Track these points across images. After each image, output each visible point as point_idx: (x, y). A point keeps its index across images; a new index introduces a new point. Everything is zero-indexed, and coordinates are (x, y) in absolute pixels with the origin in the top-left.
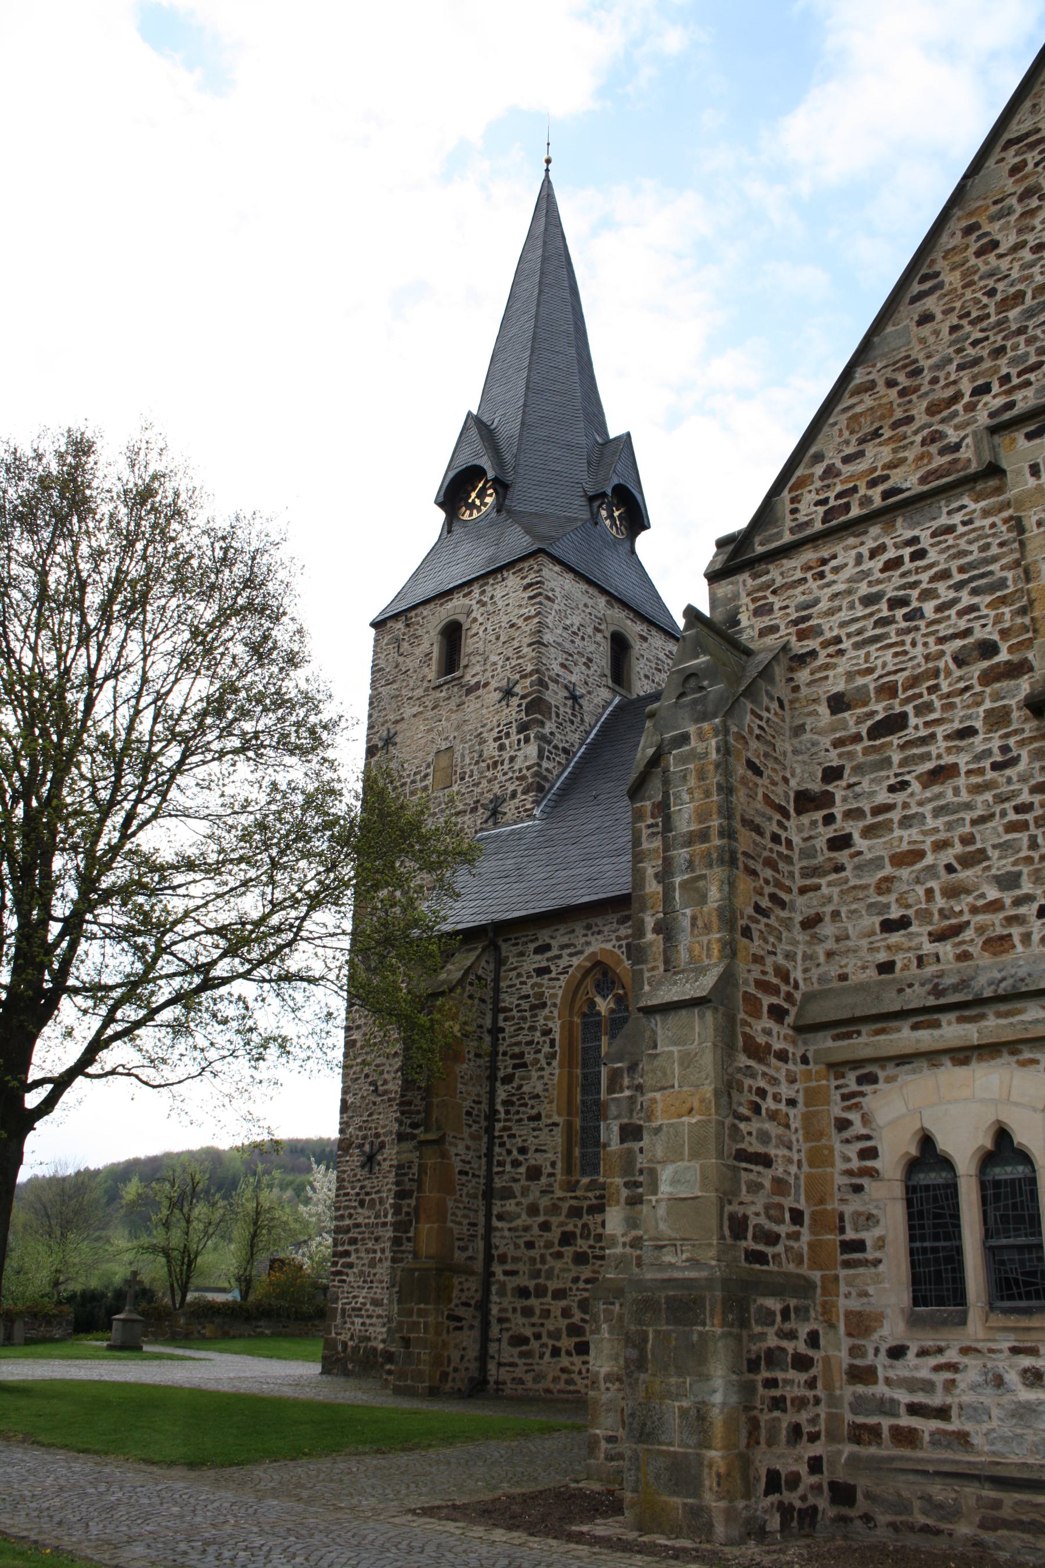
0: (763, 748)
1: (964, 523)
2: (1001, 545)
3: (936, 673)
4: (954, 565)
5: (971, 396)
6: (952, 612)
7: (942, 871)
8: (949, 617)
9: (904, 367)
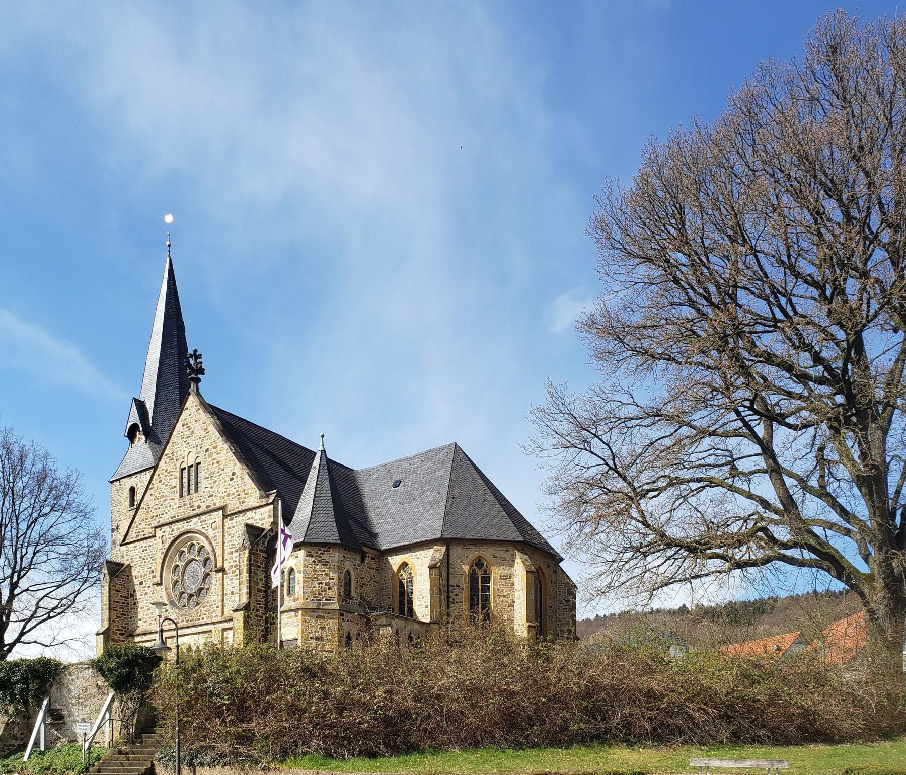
0: (120, 586)
4: (151, 553)
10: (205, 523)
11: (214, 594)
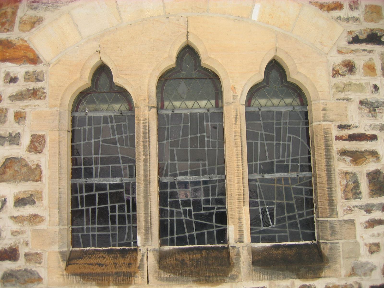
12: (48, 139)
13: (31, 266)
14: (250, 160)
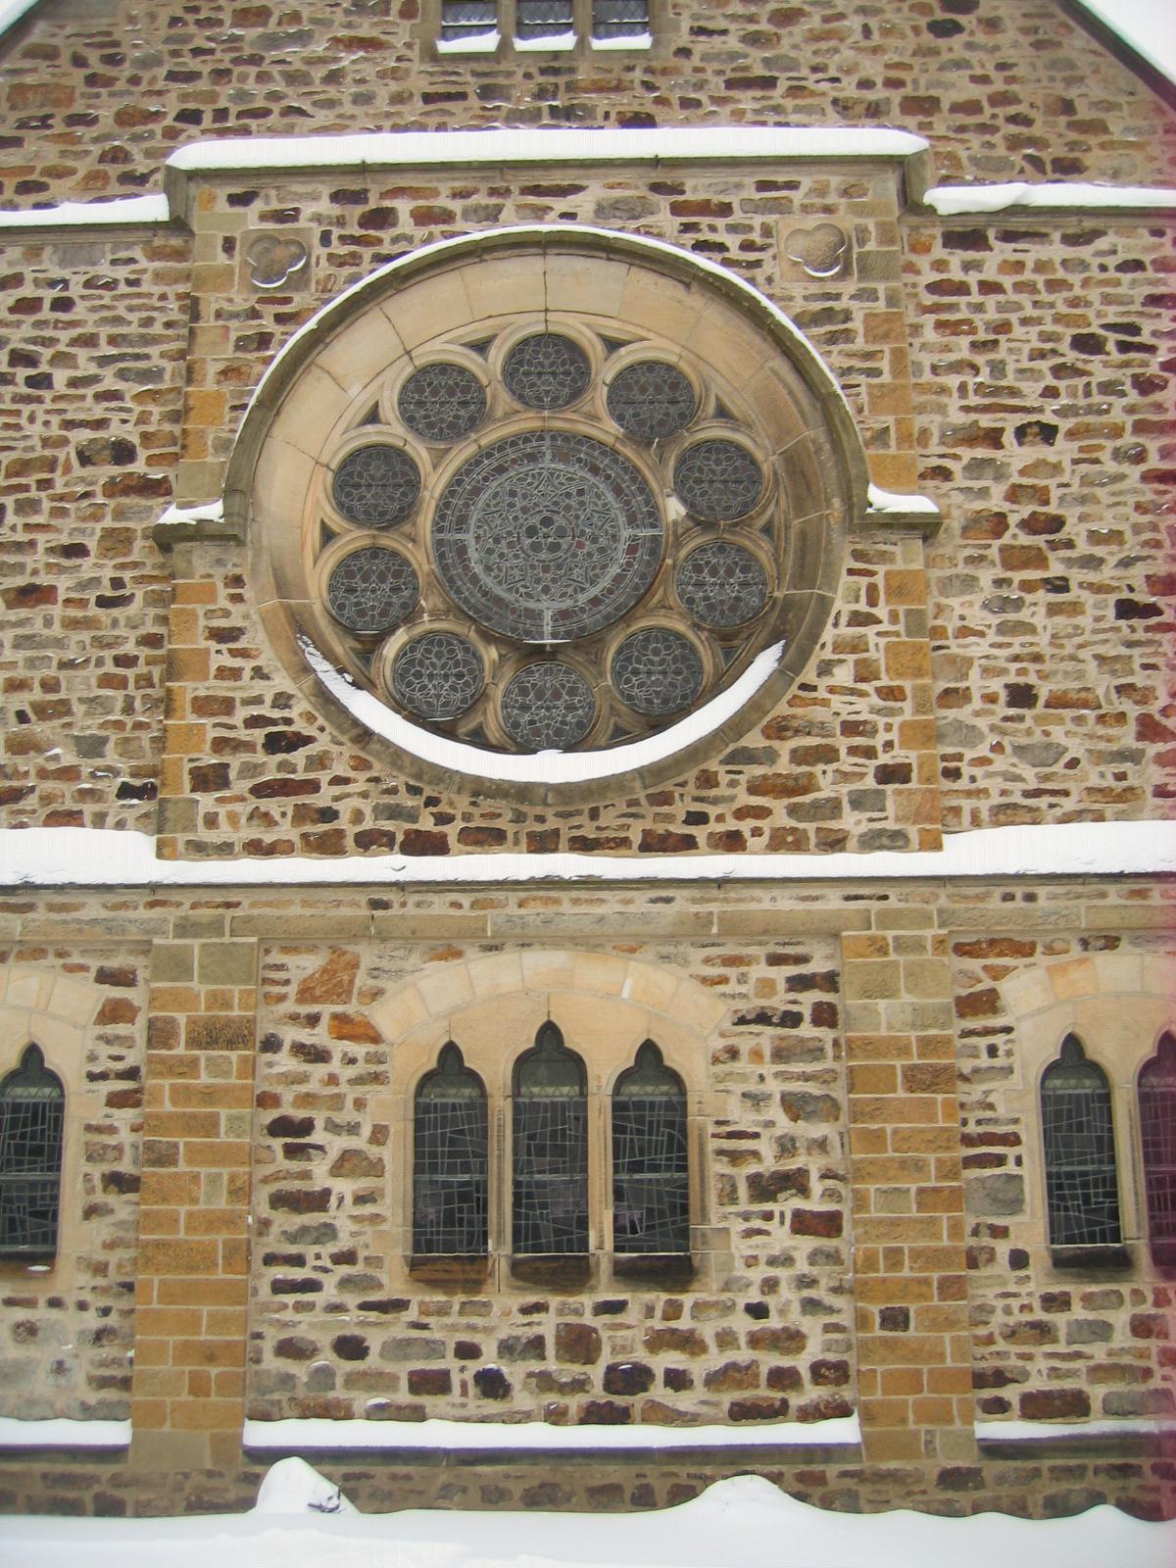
1: (130, 283)
2: (168, 325)
3: (51, 465)
4: (105, 332)
5: (176, 119)
6: (90, 392)
7: (12, 718)
8: (83, 398)
9: (102, 45)
10: (720, 223)
11: (843, 675)
12: (392, 1131)
13: (370, 1271)
14: (616, 1156)
